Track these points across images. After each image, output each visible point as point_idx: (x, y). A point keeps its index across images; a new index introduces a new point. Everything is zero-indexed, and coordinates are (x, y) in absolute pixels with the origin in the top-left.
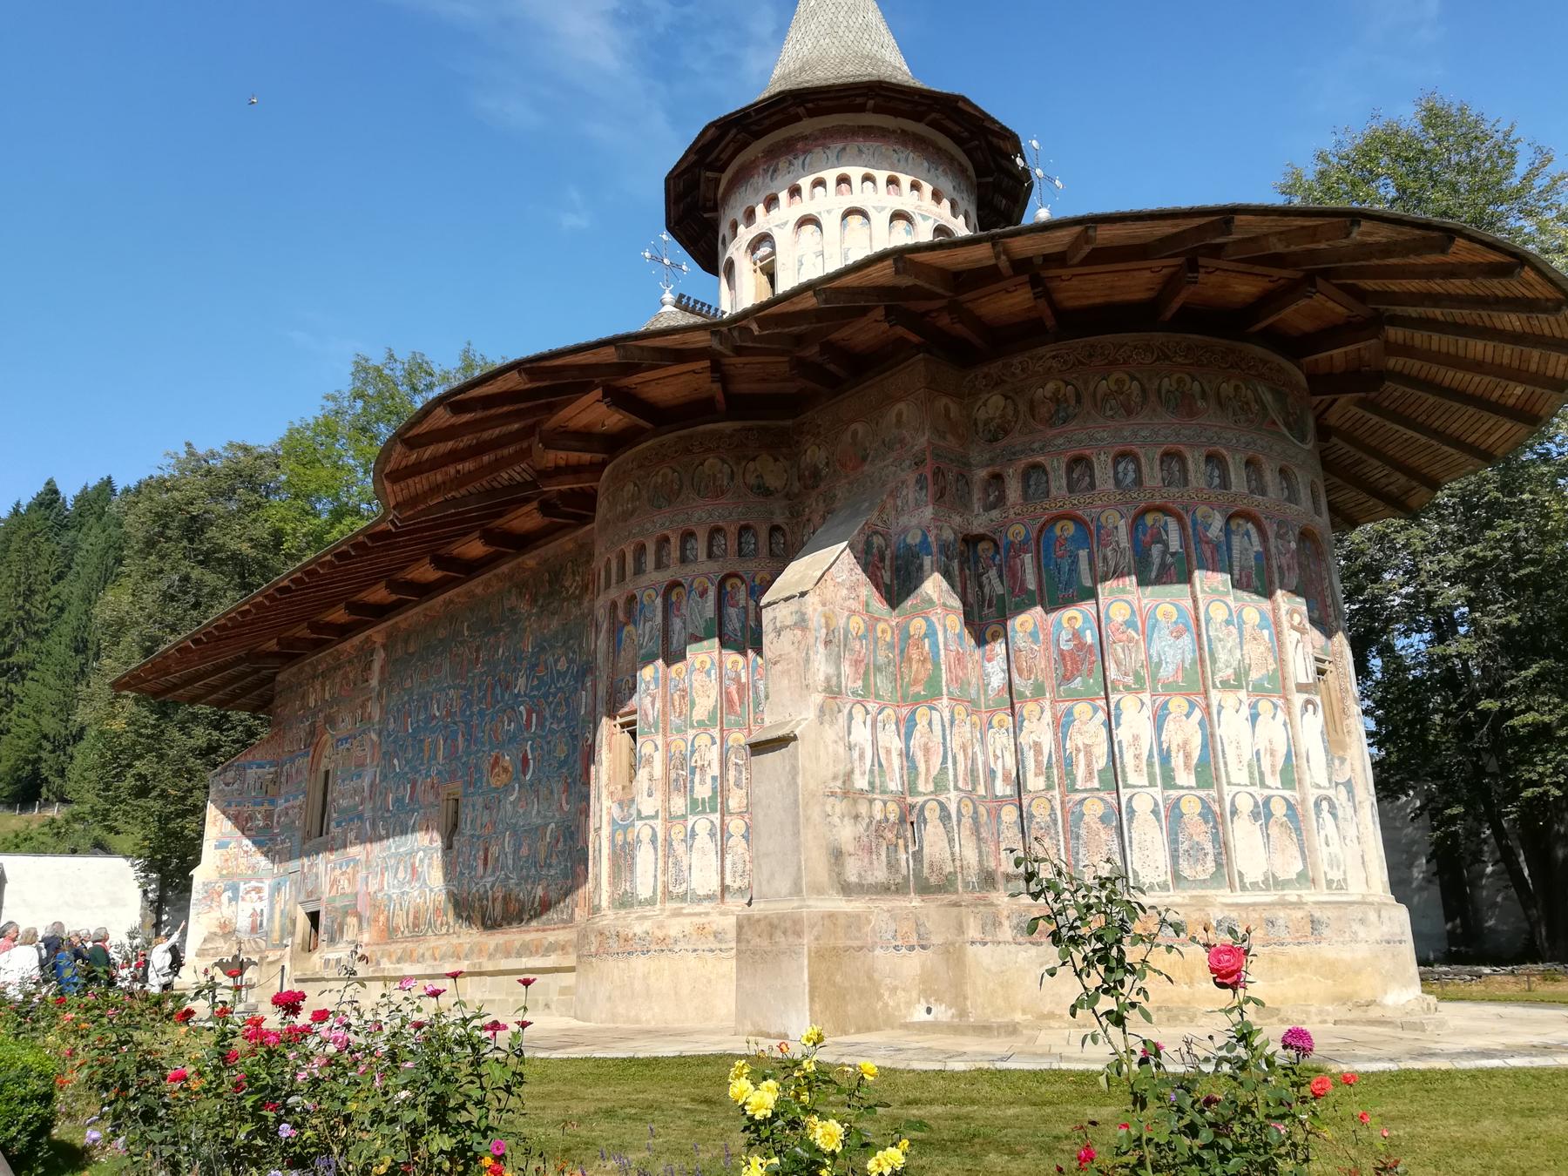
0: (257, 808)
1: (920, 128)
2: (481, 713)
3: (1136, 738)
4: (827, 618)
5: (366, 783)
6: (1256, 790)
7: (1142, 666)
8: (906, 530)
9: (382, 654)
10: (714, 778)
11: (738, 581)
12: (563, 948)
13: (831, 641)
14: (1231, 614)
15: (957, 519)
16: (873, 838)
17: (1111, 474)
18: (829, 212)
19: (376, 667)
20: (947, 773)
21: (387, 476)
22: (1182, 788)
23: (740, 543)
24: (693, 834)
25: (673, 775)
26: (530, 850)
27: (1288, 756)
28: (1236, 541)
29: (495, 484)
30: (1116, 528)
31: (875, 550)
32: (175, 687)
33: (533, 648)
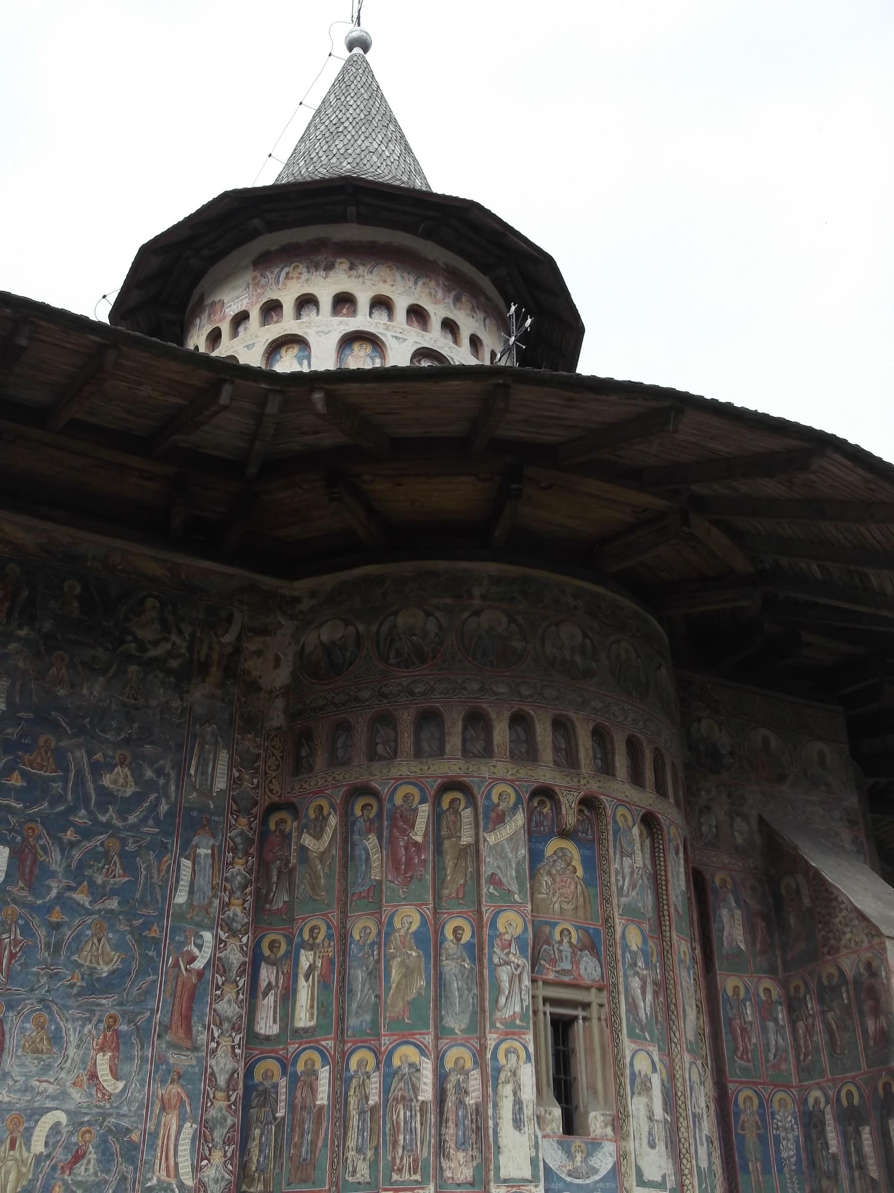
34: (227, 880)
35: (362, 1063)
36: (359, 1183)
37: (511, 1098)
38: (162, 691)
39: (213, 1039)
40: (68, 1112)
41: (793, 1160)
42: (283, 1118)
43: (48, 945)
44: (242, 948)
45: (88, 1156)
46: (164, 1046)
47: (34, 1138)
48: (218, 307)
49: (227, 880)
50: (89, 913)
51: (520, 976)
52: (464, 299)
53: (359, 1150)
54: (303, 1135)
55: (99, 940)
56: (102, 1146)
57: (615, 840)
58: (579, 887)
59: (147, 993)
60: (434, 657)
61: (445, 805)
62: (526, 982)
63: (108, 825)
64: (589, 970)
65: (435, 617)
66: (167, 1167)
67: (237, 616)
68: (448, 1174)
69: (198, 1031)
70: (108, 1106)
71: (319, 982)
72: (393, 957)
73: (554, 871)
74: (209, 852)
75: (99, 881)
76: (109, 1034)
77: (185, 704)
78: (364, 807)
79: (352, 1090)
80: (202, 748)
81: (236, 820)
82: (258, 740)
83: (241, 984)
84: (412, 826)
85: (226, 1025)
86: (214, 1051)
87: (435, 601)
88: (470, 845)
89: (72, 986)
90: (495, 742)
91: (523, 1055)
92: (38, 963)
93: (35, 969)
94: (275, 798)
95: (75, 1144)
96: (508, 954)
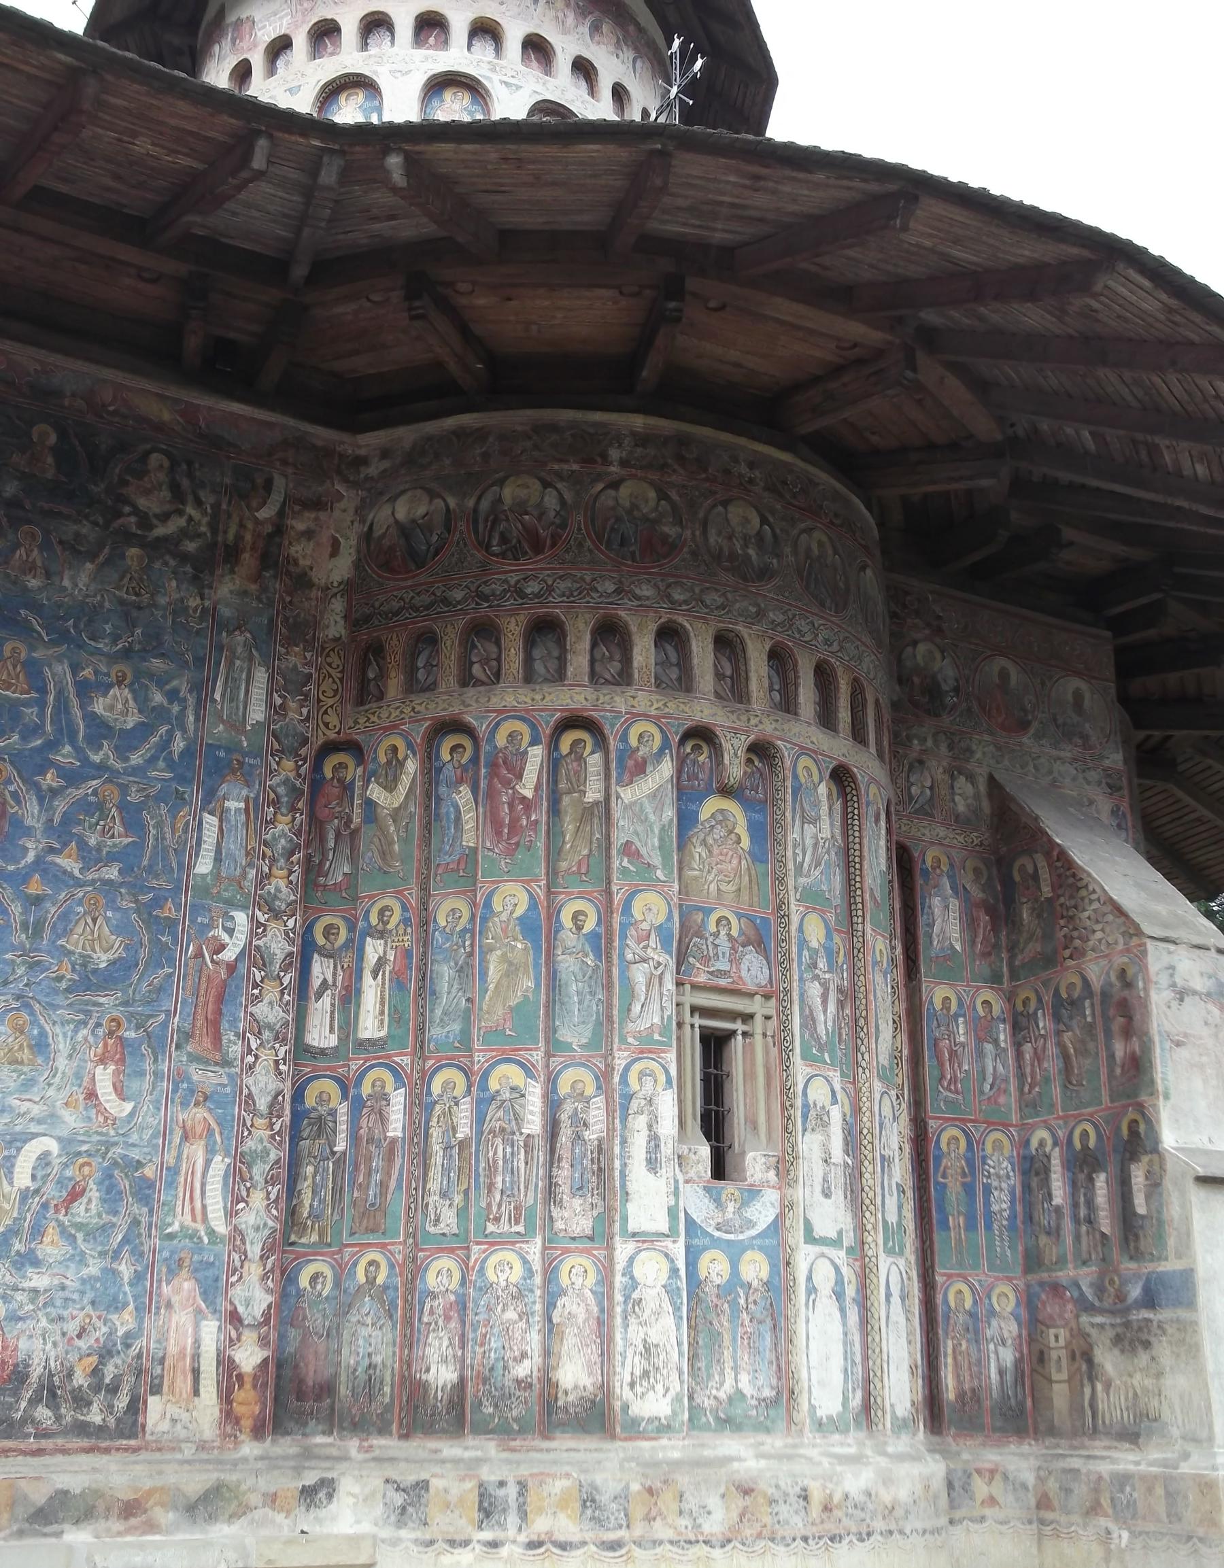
12: (130, 1509)
34: (266, 844)
35: (448, 1085)
36: (444, 1235)
37: (645, 1132)
38: (174, 583)
39: (250, 1051)
40: (59, 1139)
41: (1005, 1214)
42: (344, 1153)
43: (25, 926)
44: (287, 934)
45: (87, 1194)
46: (185, 1059)
47: (17, 1170)
48: (246, 27)
49: (266, 844)
50: (80, 884)
51: (661, 977)
52: (605, 28)
53: (444, 1195)
54: (370, 1174)
55: (94, 920)
56: (107, 1183)
57: (794, 801)
58: (744, 862)
59: (160, 990)
60: (553, 545)
61: (565, 747)
62: (669, 985)
63: (102, 767)
64: (753, 972)
65: (556, 489)
66: (193, 1210)
67: (279, 482)
68: (560, 1225)
69: (230, 1041)
70: (112, 1133)
71: (391, 980)
72: (491, 949)
73: (710, 841)
74: (242, 805)
75: (92, 842)
76: (111, 1042)
77: (207, 603)
78: (453, 749)
79: (435, 1120)
80: (231, 664)
81: (278, 764)
82: (308, 655)
83: (286, 981)
84: (520, 777)
85: (267, 1034)
86: (251, 1067)
87: (556, 467)
88: (597, 803)
89: (60, 979)
90: (635, 664)
91: (662, 1078)
92: (13, 948)
93: (8, 956)
94: (332, 735)
95: (71, 1179)
96: (646, 947)
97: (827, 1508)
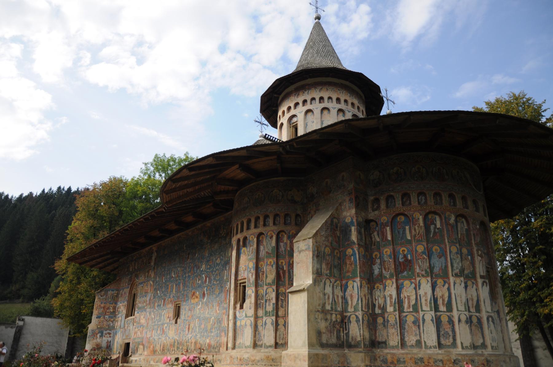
0: (110, 305)
1: (347, 83)
2: (189, 276)
3: (426, 293)
4: (318, 248)
5: (148, 299)
6: (467, 313)
7: (428, 268)
8: (345, 217)
9: (156, 254)
10: (273, 304)
11: (284, 234)
13: (319, 256)
14: (458, 250)
15: (363, 214)
16: (332, 327)
17: (417, 200)
18: (317, 108)
19: (153, 258)
20: (359, 305)
21: (165, 192)
22: (441, 312)
23: (285, 220)
24: (266, 324)
25: (259, 302)
26: (205, 326)
27: (478, 301)
28: (459, 224)
29: (199, 196)
30: (419, 219)
31: (334, 224)
32: (87, 262)
33: (208, 255)
57: (249, 243)
63: (217, 269)
97: (240, 360)
